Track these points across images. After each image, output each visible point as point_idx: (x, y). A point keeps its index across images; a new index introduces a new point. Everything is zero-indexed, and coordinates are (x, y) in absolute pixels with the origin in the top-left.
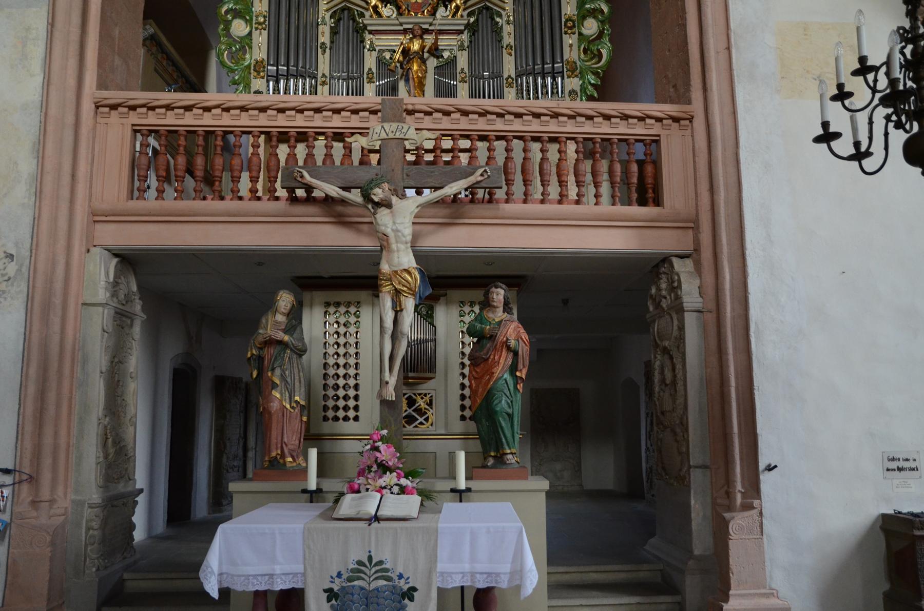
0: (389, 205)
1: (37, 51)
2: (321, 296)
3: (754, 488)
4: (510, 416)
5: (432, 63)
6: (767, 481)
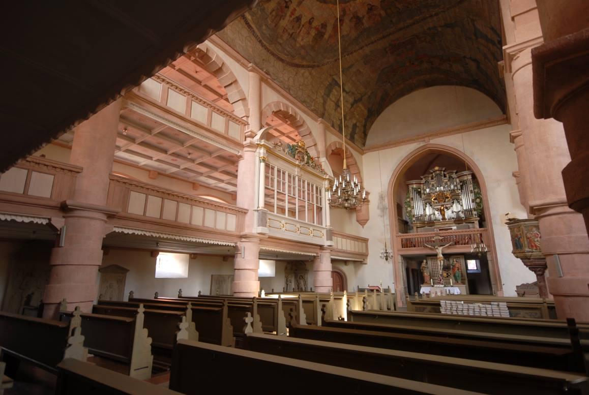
0: (437, 248)
1: (389, 231)
2: (430, 257)
3: (501, 288)
4: (459, 276)
5: (445, 210)
6: (503, 286)
